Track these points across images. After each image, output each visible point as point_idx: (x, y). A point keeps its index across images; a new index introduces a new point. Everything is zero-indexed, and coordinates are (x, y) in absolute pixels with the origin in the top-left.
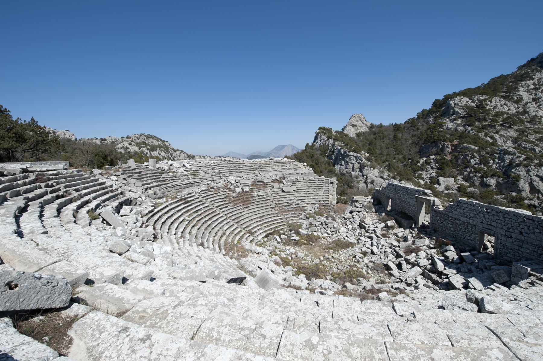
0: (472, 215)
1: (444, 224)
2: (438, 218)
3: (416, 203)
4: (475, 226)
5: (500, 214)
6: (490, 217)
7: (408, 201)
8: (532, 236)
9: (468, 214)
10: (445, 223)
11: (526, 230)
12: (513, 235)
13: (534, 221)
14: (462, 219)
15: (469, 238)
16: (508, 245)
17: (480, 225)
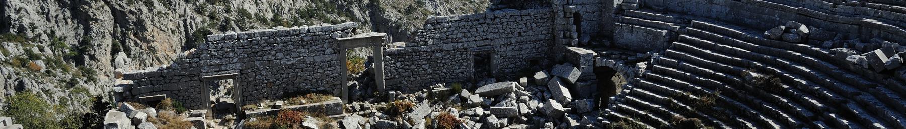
0: (460, 35)
1: (412, 70)
2: (398, 64)
3: (335, 57)
4: (466, 49)
5: (498, 20)
6: (486, 28)
7: (308, 60)
8: (531, 33)
9: (454, 36)
10: (413, 67)
11: (525, 29)
12: (513, 40)
13: (530, 15)
14: (445, 47)
15: (458, 71)
16: (509, 54)
17: (473, 45)
